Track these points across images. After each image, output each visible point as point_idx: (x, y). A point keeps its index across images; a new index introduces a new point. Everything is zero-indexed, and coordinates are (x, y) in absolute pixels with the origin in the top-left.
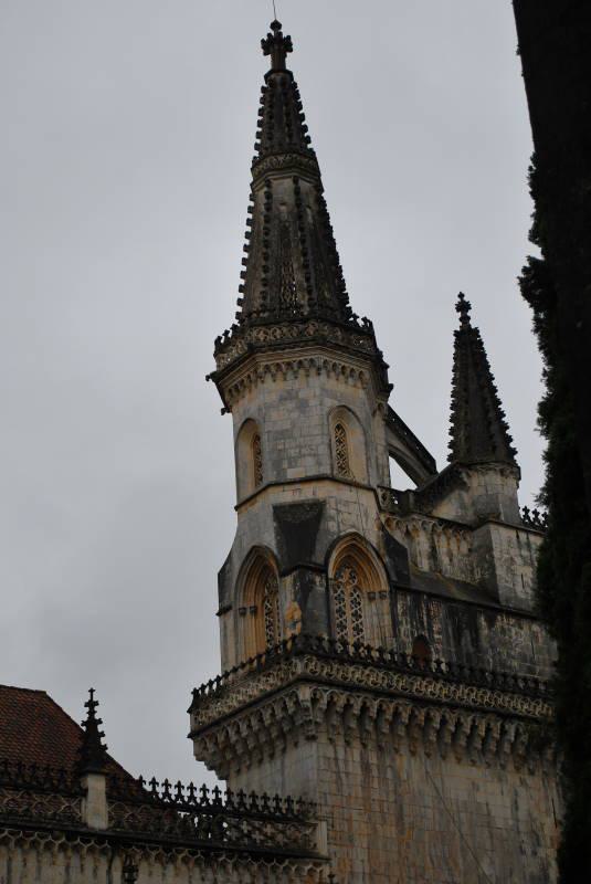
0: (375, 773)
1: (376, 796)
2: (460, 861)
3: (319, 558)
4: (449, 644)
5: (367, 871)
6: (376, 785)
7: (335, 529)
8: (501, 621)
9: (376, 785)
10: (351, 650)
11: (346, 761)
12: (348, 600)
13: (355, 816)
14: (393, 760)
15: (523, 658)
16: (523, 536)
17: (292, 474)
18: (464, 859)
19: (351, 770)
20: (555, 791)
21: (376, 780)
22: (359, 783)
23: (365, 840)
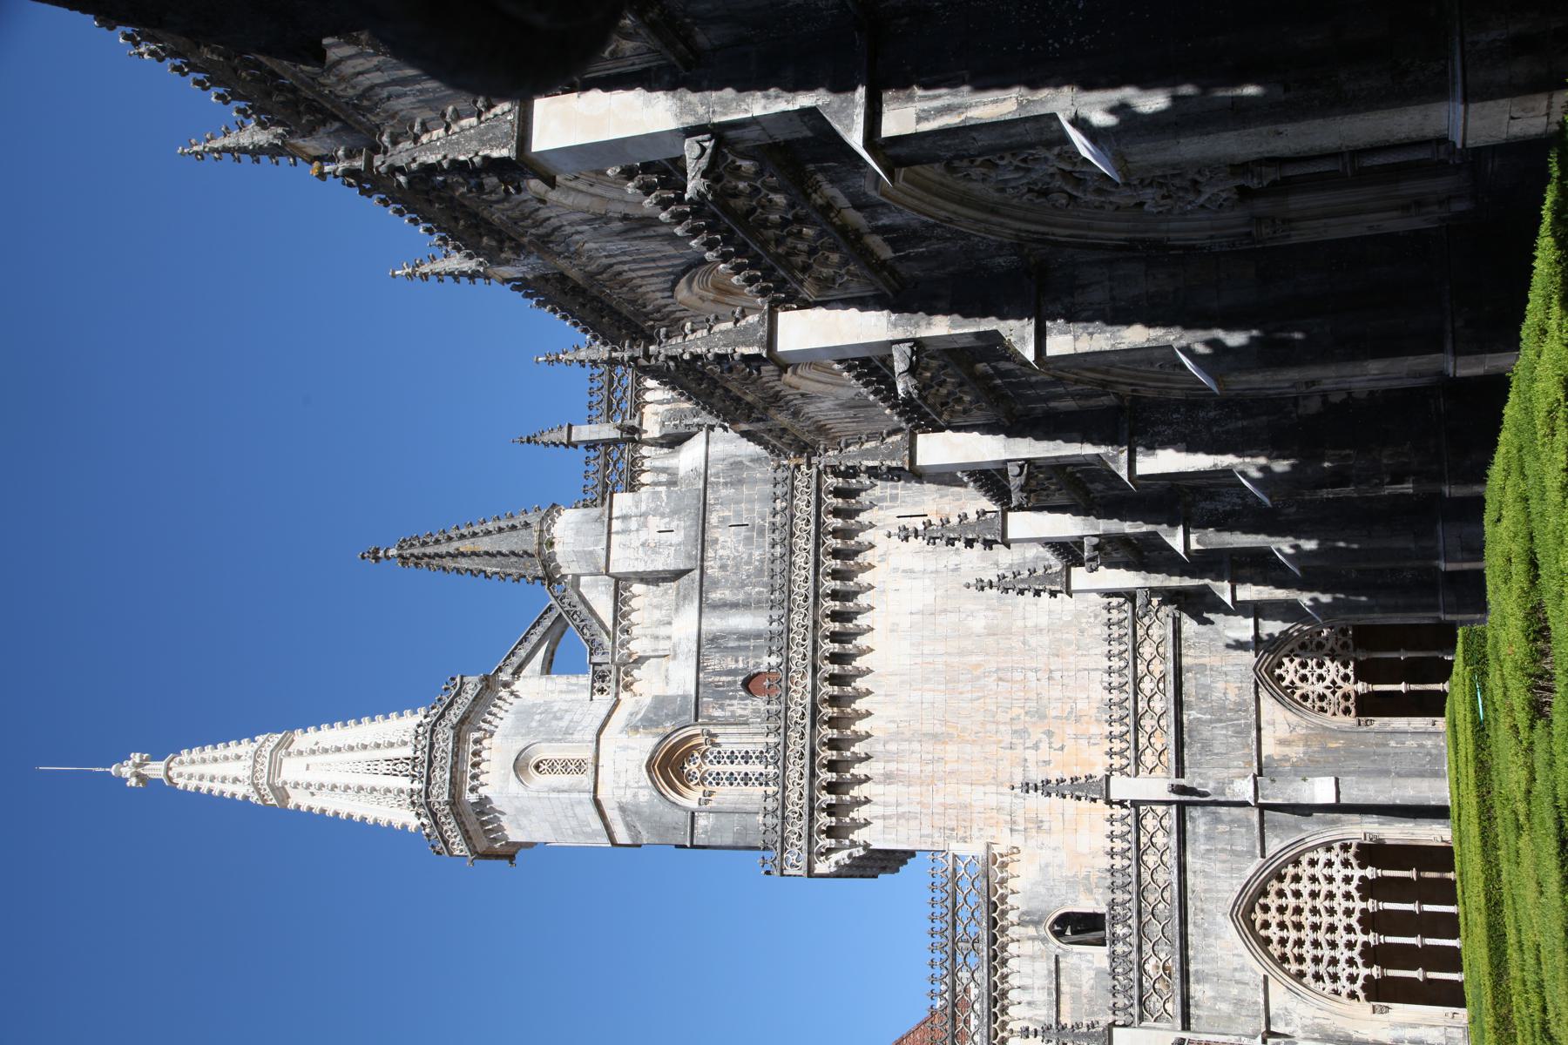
0: (892, 767)
1: (916, 768)
2: (974, 659)
3: (684, 818)
4: (747, 648)
5: (993, 789)
6: (904, 767)
7: (646, 792)
8: (713, 570)
9: (904, 767)
10: (771, 789)
11: (885, 805)
12: (716, 768)
13: (939, 799)
14: (878, 740)
15: (748, 540)
16: (616, 525)
17: (597, 824)
18: (971, 653)
19: (892, 800)
20: (888, 512)
21: (901, 766)
22: (904, 789)
23: (963, 787)
